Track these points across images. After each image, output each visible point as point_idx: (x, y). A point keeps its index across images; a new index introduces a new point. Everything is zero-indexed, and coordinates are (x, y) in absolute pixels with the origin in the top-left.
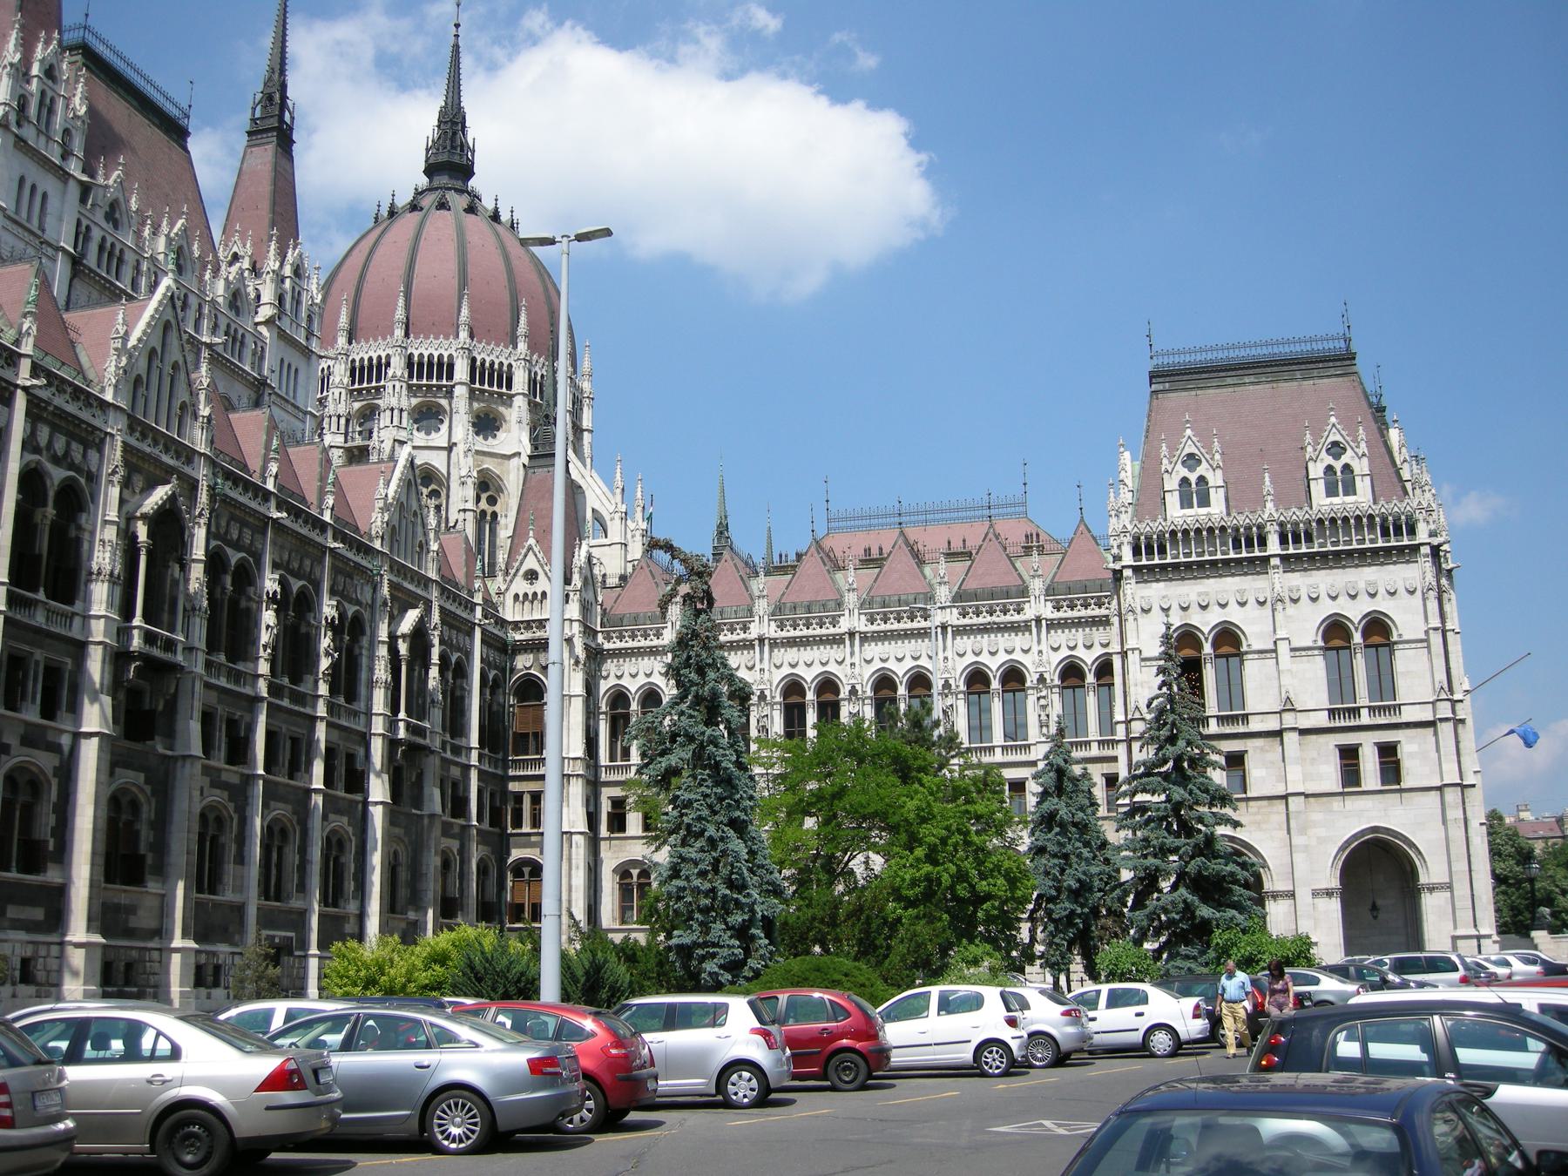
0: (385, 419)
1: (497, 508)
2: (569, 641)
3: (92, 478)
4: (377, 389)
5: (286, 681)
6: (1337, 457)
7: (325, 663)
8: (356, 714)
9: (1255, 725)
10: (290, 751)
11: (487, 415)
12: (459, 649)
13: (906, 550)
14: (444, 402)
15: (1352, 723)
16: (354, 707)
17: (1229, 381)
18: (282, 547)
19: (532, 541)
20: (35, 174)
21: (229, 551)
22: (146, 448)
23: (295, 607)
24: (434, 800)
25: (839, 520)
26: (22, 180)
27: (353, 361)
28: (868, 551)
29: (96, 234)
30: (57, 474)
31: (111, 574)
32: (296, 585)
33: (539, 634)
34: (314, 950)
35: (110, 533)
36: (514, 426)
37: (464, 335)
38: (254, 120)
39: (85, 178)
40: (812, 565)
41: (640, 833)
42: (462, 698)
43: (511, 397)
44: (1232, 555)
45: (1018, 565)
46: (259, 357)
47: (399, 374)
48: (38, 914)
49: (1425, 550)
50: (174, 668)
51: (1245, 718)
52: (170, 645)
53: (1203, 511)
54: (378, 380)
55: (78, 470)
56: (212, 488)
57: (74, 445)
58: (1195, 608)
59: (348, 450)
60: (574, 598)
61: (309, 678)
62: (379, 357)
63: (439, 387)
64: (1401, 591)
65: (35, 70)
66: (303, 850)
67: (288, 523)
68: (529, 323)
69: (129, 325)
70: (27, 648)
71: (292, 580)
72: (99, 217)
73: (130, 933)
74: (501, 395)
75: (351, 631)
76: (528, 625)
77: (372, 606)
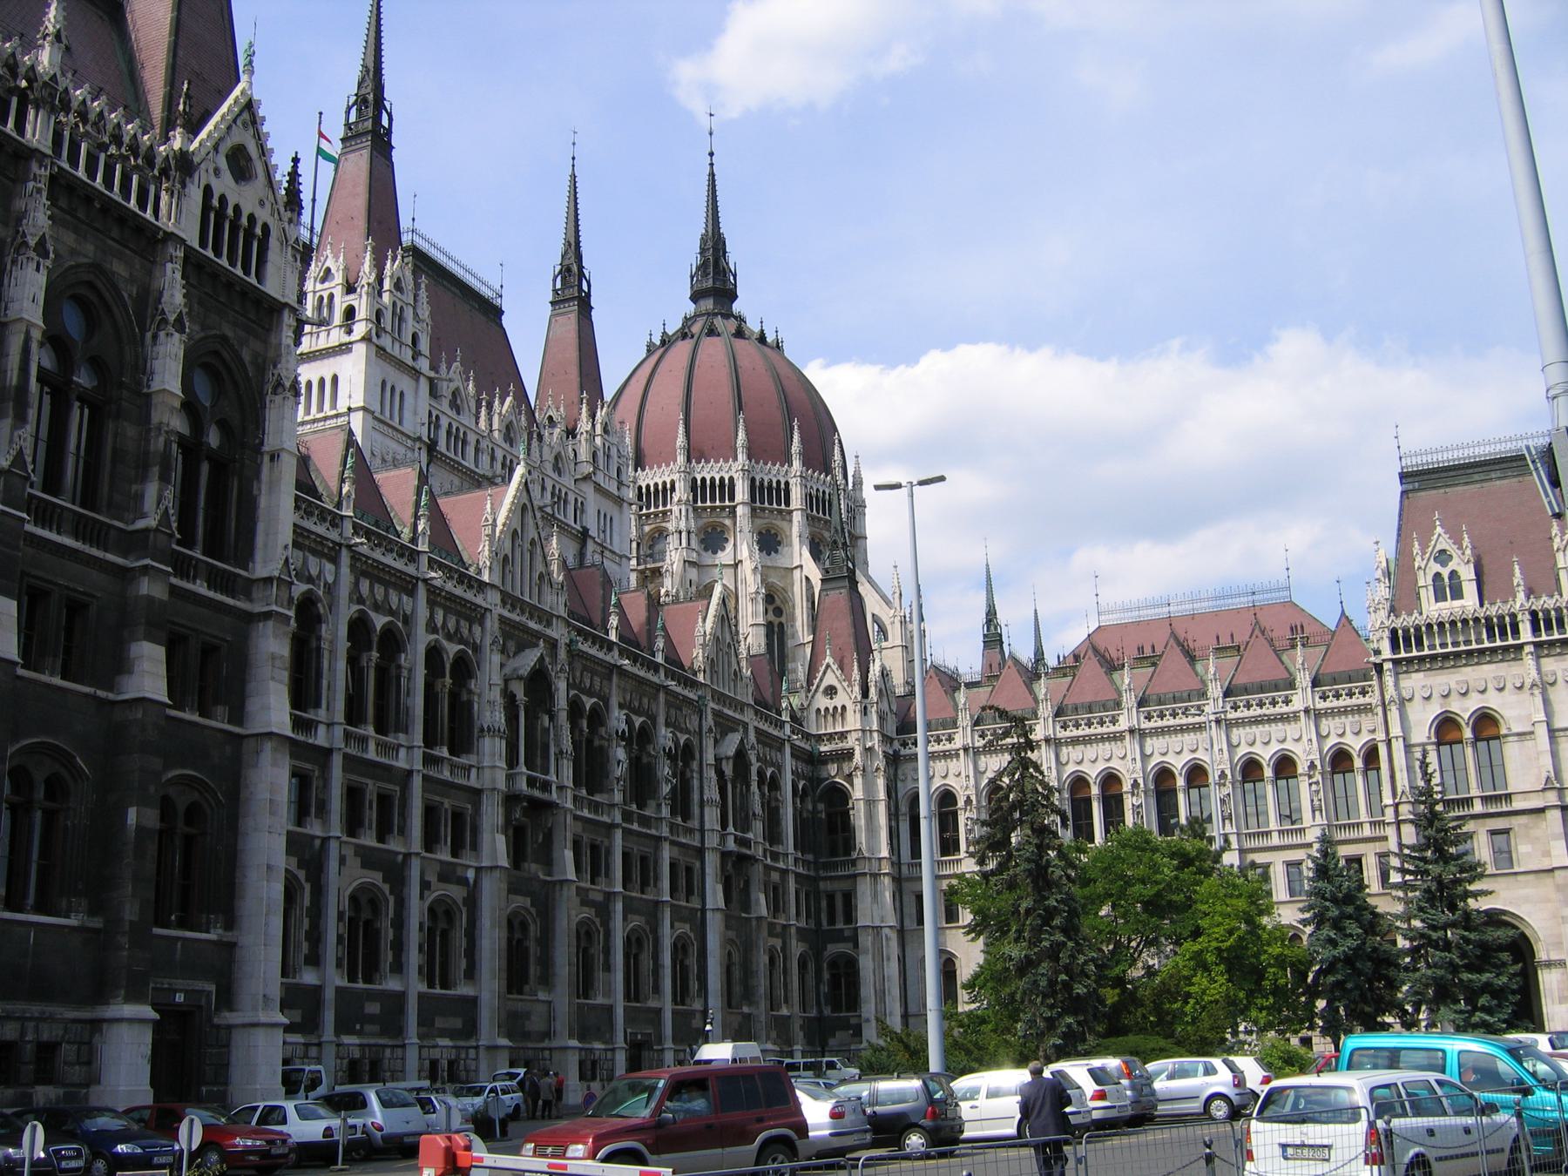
0: (673, 541)
1: (783, 620)
3: (477, 648)
4: (664, 513)
5: (634, 807)
8: (691, 831)
9: (1517, 804)
10: (641, 869)
11: (768, 531)
12: (773, 765)
13: (1178, 650)
14: (728, 522)
16: (689, 824)
17: (1476, 477)
18: (624, 690)
19: (829, 660)
21: (584, 698)
22: (514, 617)
23: (640, 738)
24: (761, 904)
25: (1109, 612)
26: (384, 383)
27: (640, 488)
28: (1141, 649)
29: (444, 422)
30: (452, 649)
32: (638, 721)
34: (669, 1044)
35: (496, 695)
36: (796, 541)
37: (742, 457)
38: (555, 291)
39: (432, 374)
40: (1091, 666)
42: (777, 808)
44: (1487, 644)
45: (1285, 658)
46: (580, 509)
47: (684, 498)
48: (457, 1023)
50: (550, 805)
51: (1508, 797)
52: (546, 786)
53: (1457, 603)
54: (665, 504)
55: (466, 643)
57: (462, 623)
59: (642, 572)
61: (652, 803)
62: (664, 483)
63: (723, 508)
65: (387, 285)
66: (656, 957)
67: (629, 668)
68: (803, 441)
69: (494, 512)
70: (437, 798)
71: (634, 717)
72: (445, 406)
73: (526, 1036)
74: (780, 512)
75: (684, 755)
76: (831, 737)
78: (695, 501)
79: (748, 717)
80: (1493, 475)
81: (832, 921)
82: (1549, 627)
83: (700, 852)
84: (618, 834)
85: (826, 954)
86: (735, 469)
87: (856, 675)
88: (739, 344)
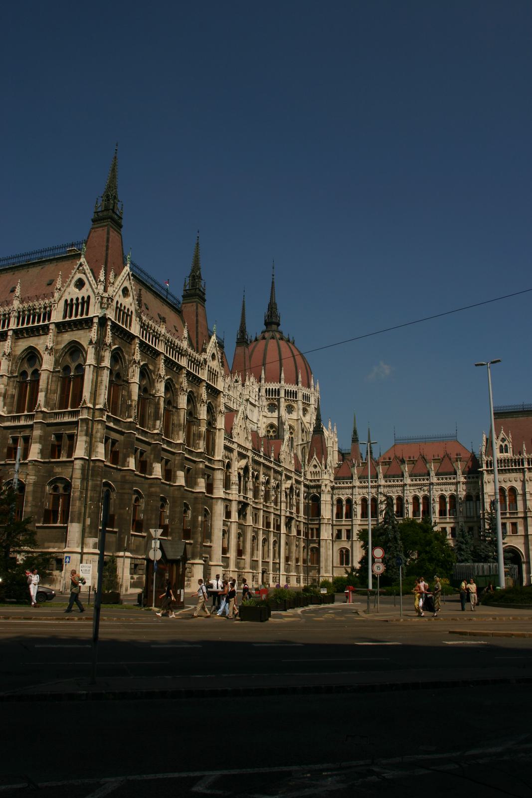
8: (277, 510)
16: (277, 508)
35: (236, 473)
41: (346, 539)
45: (454, 465)
53: (506, 454)
76: (315, 481)
77: (281, 481)
78: (266, 396)
79: (293, 475)
80: (520, 416)
81: (312, 536)
83: (280, 516)
84: (262, 511)
85: (310, 547)
87: (323, 462)
88: (281, 342)
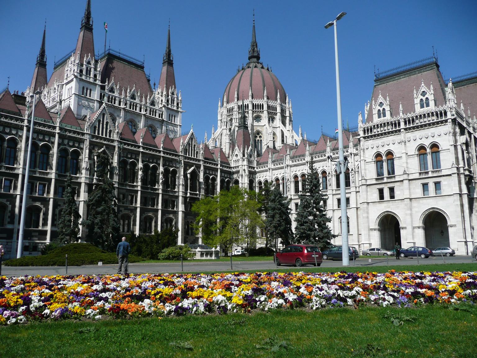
0: (233, 120)
2: (244, 170)
3: (82, 149)
6: (424, 96)
7: (161, 181)
15: (427, 176)
20: (86, 85)
31: (86, 168)
33: (238, 169)
38: (164, 60)
39: (101, 84)
43: (263, 111)
46: (161, 115)
49: (450, 120)
53: (385, 118)
56: (119, 147)
58: (380, 147)
60: (246, 160)
64: (443, 134)
74: (260, 111)
76: (236, 167)
79: (201, 163)
82: (409, 123)
86: (264, 102)
87: (242, 151)
88: (255, 69)
